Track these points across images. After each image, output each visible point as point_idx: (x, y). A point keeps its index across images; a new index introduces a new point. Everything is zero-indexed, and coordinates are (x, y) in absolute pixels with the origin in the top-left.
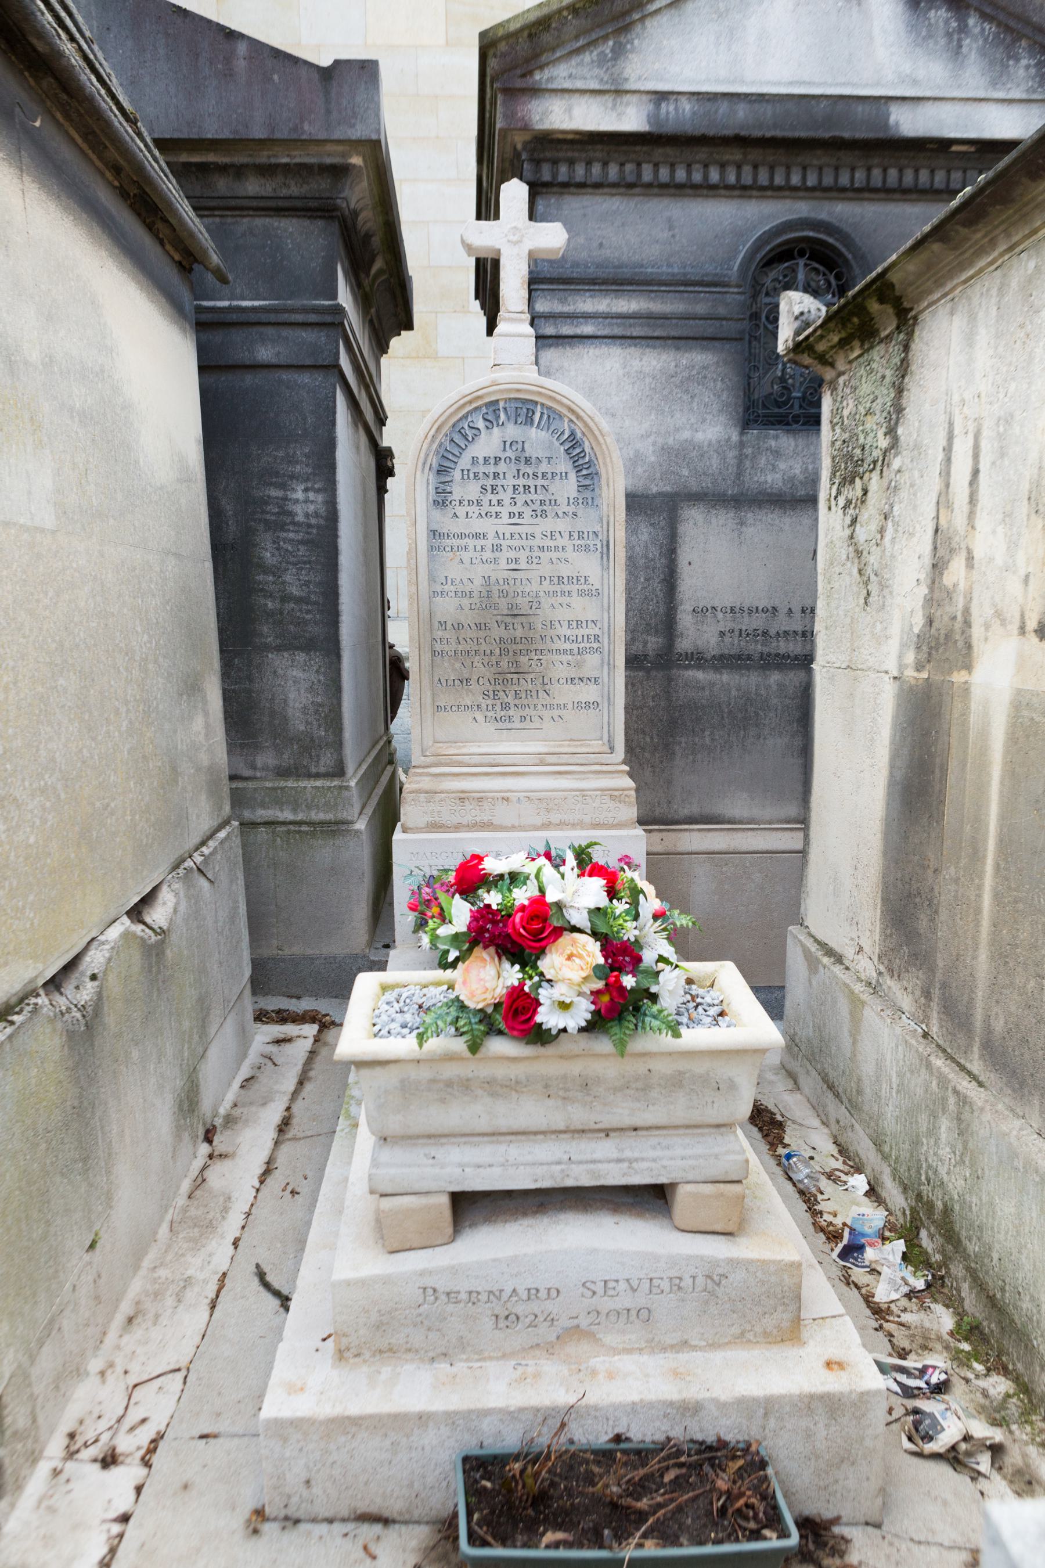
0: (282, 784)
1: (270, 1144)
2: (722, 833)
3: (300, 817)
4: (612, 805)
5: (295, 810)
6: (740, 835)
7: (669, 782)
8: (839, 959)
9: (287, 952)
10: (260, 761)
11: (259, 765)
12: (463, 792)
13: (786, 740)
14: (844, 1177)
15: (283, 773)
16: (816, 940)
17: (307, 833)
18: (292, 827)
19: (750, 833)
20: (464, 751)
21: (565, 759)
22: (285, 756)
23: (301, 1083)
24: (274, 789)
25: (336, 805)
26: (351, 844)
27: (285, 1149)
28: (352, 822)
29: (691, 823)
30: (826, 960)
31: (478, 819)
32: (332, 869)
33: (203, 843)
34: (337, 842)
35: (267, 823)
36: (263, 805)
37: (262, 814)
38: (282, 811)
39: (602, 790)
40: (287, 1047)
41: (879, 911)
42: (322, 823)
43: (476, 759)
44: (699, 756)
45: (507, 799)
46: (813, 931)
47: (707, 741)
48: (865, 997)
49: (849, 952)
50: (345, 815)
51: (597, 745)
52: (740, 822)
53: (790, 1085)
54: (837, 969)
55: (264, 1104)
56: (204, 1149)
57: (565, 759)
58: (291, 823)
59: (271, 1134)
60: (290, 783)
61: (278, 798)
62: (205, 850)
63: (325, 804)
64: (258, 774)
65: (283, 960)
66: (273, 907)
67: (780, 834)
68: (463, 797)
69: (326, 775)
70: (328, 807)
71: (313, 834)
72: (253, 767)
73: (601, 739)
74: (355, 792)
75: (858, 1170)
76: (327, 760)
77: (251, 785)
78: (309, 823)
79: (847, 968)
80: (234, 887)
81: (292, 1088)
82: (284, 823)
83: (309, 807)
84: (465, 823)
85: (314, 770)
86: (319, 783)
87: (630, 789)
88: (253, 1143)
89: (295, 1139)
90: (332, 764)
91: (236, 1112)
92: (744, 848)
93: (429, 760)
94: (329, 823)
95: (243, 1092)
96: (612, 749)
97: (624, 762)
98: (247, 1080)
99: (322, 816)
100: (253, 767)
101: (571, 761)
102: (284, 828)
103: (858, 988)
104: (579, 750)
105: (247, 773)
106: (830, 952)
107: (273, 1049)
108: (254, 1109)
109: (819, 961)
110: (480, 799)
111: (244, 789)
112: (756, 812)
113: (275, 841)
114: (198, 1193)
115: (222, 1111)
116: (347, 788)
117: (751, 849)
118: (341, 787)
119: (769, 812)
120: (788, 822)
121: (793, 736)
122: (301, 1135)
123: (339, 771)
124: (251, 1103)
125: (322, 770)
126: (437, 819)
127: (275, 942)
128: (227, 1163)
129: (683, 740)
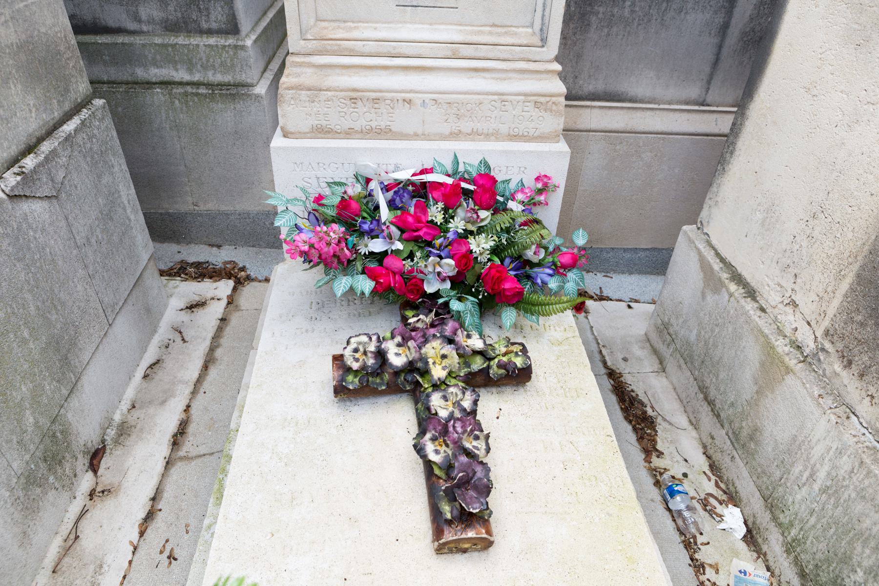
0: (172, 40)
1: (160, 466)
2: (622, 112)
3: (197, 77)
4: (535, 113)
5: (190, 70)
6: (639, 114)
7: (579, 56)
8: (752, 294)
9: (202, 207)
10: (144, 12)
11: (144, 17)
12: (355, 90)
13: (708, 16)
14: (720, 509)
15: (172, 27)
16: (718, 254)
17: (205, 96)
18: (189, 89)
19: (649, 113)
20: (355, 34)
21: (484, 51)
22: (171, 8)
23: (206, 367)
24: (164, 46)
25: (233, 66)
26: (253, 108)
27: (176, 471)
28: (252, 86)
29: (593, 100)
30: (733, 287)
31: (374, 124)
32: (236, 132)
33: (30, 149)
34: (238, 106)
35: (166, 84)
36: (155, 64)
37: (155, 73)
38: (177, 70)
39: (526, 95)
40: (200, 313)
41: (845, 286)
42: (221, 85)
43: (371, 47)
44: (615, 29)
45: (409, 102)
46: (714, 242)
47: (626, 12)
48: (792, 363)
49: (771, 297)
50: (243, 77)
51: (525, 34)
52: (641, 101)
53: (656, 366)
54: (749, 306)
55: (164, 402)
56: (86, 481)
57: (484, 51)
58: (188, 84)
59: (164, 450)
60: (181, 40)
61: (170, 56)
62: (29, 162)
63: (222, 64)
64: (145, 28)
65: (201, 215)
66: (182, 168)
67: (677, 115)
68: (355, 97)
69: (219, 32)
70: (226, 68)
71: (212, 97)
72: (140, 21)
73: (532, 25)
74: (251, 52)
75: (733, 498)
76: (217, 16)
77: (138, 40)
78: (208, 85)
79: (763, 310)
80: (106, 179)
81: (196, 375)
82: (181, 84)
83: (205, 68)
84: (358, 128)
85: (205, 26)
86: (212, 41)
87: (559, 95)
88: (139, 466)
89: (187, 458)
90: (224, 19)
91: (131, 420)
92: (641, 128)
93: (311, 45)
94: (229, 84)
95: (145, 385)
96: (544, 41)
97: (557, 59)
98: (151, 366)
99: (219, 78)
100: (140, 21)
101: (490, 55)
102: (180, 90)
103: (781, 346)
104: (502, 40)
105: (132, 26)
106: (738, 278)
107: (185, 317)
108: (151, 410)
109: (722, 284)
110: (376, 100)
111: (131, 45)
112: (659, 92)
113: (173, 103)
114: (66, 560)
115: (117, 417)
116: (243, 48)
117: (647, 129)
118: (236, 47)
119: (673, 92)
120: (687, 103)
121: (716, 12)
122: (194, 452)
123: (233, 29)
124: (150, 402)
125: (214, 26)
126: (324, 123)
127: (190, 199)
128: (110, 503)
129: (601, 10)
